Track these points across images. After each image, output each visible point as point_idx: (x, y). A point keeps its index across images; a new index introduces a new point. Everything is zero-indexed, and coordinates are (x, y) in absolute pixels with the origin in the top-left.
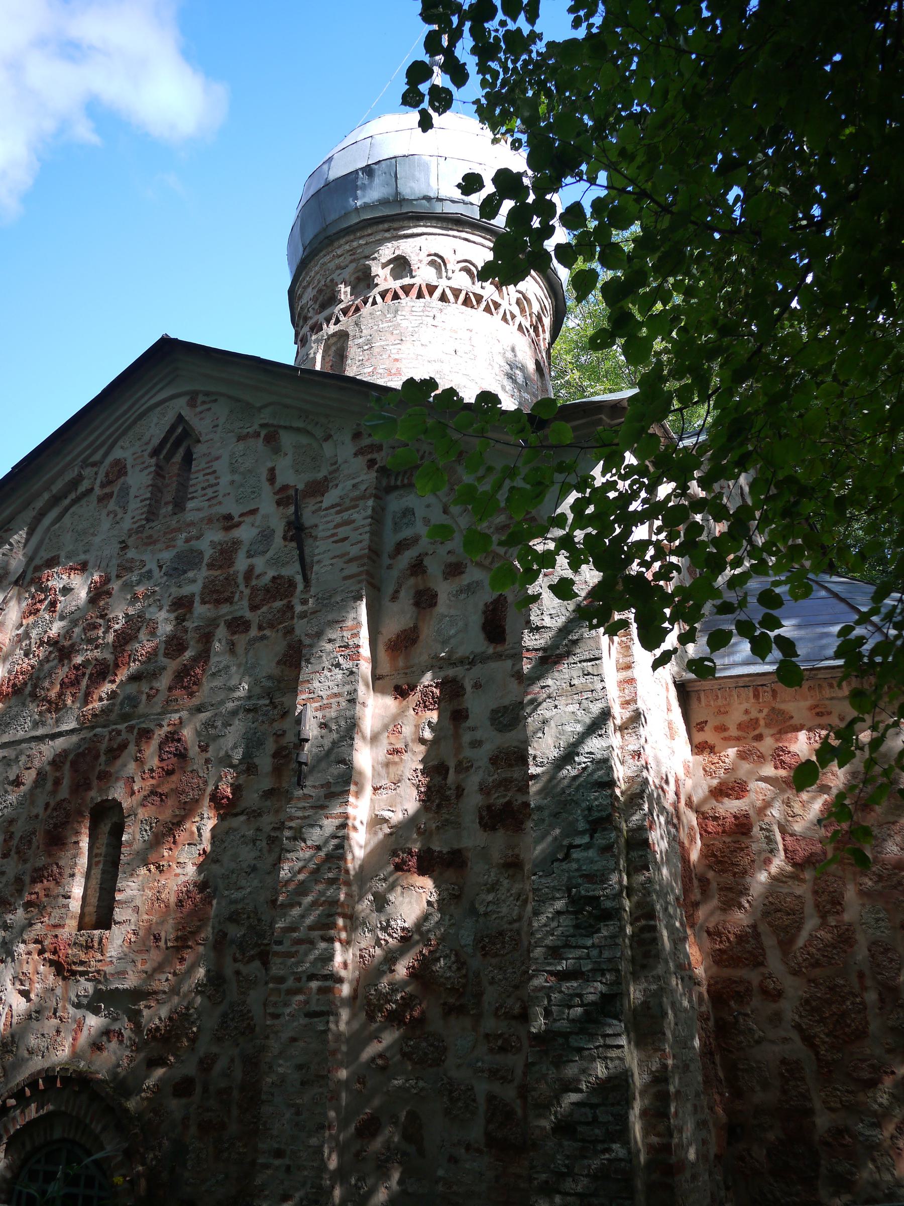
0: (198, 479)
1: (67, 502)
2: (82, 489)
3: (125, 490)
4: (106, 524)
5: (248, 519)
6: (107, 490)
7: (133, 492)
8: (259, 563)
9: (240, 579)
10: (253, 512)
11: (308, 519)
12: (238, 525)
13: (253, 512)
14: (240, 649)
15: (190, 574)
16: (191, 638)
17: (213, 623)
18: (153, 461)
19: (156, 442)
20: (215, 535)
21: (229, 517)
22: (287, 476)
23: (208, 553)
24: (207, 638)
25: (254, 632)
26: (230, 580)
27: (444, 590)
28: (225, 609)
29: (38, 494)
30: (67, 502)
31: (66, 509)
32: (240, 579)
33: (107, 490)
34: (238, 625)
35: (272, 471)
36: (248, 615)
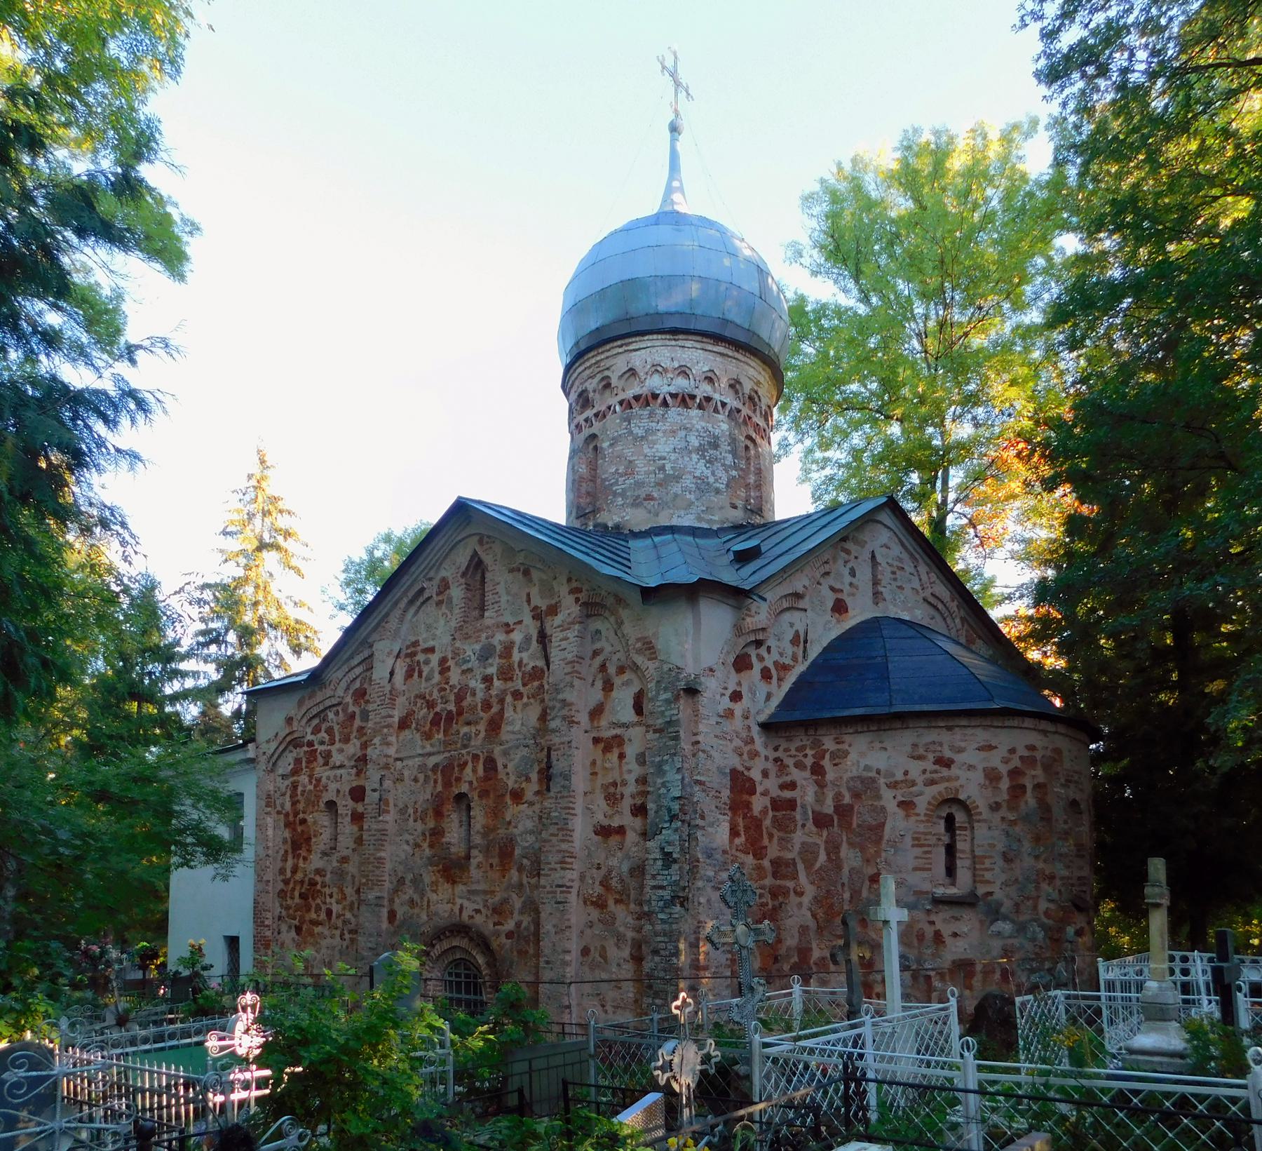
0: (489, 598)
1: (418, 603)
2: (426, 595)
3: (450, 599)
4: (442, 622)
5: (518, 627)
6: (440, 598)
7: (455, 601)
8: (525, 655)
9: (516, 666)
10: (520, 622)
11: (549, 631)
12: (512, 630)
13: (520, 622)
14: (519, 709)
15: (490, 661)
16: (494, 701)
17: (504, 692)
18: (463, 581)
19: (463, 568)
20: (500, 637)
21: (507, 625)
22: (537, 601)
23: (499, 648)
24: (502, 701)
25: (525, 700)
26: (511, 667)
27: (618, 681)
28: (510, 684)
29: (401, 599)
30: (418, 603)
31: (420, 607)
32: (516, 666)
33: (440, 598)
34: (517, 695)
35: (528, 595)
36: (521, 689)
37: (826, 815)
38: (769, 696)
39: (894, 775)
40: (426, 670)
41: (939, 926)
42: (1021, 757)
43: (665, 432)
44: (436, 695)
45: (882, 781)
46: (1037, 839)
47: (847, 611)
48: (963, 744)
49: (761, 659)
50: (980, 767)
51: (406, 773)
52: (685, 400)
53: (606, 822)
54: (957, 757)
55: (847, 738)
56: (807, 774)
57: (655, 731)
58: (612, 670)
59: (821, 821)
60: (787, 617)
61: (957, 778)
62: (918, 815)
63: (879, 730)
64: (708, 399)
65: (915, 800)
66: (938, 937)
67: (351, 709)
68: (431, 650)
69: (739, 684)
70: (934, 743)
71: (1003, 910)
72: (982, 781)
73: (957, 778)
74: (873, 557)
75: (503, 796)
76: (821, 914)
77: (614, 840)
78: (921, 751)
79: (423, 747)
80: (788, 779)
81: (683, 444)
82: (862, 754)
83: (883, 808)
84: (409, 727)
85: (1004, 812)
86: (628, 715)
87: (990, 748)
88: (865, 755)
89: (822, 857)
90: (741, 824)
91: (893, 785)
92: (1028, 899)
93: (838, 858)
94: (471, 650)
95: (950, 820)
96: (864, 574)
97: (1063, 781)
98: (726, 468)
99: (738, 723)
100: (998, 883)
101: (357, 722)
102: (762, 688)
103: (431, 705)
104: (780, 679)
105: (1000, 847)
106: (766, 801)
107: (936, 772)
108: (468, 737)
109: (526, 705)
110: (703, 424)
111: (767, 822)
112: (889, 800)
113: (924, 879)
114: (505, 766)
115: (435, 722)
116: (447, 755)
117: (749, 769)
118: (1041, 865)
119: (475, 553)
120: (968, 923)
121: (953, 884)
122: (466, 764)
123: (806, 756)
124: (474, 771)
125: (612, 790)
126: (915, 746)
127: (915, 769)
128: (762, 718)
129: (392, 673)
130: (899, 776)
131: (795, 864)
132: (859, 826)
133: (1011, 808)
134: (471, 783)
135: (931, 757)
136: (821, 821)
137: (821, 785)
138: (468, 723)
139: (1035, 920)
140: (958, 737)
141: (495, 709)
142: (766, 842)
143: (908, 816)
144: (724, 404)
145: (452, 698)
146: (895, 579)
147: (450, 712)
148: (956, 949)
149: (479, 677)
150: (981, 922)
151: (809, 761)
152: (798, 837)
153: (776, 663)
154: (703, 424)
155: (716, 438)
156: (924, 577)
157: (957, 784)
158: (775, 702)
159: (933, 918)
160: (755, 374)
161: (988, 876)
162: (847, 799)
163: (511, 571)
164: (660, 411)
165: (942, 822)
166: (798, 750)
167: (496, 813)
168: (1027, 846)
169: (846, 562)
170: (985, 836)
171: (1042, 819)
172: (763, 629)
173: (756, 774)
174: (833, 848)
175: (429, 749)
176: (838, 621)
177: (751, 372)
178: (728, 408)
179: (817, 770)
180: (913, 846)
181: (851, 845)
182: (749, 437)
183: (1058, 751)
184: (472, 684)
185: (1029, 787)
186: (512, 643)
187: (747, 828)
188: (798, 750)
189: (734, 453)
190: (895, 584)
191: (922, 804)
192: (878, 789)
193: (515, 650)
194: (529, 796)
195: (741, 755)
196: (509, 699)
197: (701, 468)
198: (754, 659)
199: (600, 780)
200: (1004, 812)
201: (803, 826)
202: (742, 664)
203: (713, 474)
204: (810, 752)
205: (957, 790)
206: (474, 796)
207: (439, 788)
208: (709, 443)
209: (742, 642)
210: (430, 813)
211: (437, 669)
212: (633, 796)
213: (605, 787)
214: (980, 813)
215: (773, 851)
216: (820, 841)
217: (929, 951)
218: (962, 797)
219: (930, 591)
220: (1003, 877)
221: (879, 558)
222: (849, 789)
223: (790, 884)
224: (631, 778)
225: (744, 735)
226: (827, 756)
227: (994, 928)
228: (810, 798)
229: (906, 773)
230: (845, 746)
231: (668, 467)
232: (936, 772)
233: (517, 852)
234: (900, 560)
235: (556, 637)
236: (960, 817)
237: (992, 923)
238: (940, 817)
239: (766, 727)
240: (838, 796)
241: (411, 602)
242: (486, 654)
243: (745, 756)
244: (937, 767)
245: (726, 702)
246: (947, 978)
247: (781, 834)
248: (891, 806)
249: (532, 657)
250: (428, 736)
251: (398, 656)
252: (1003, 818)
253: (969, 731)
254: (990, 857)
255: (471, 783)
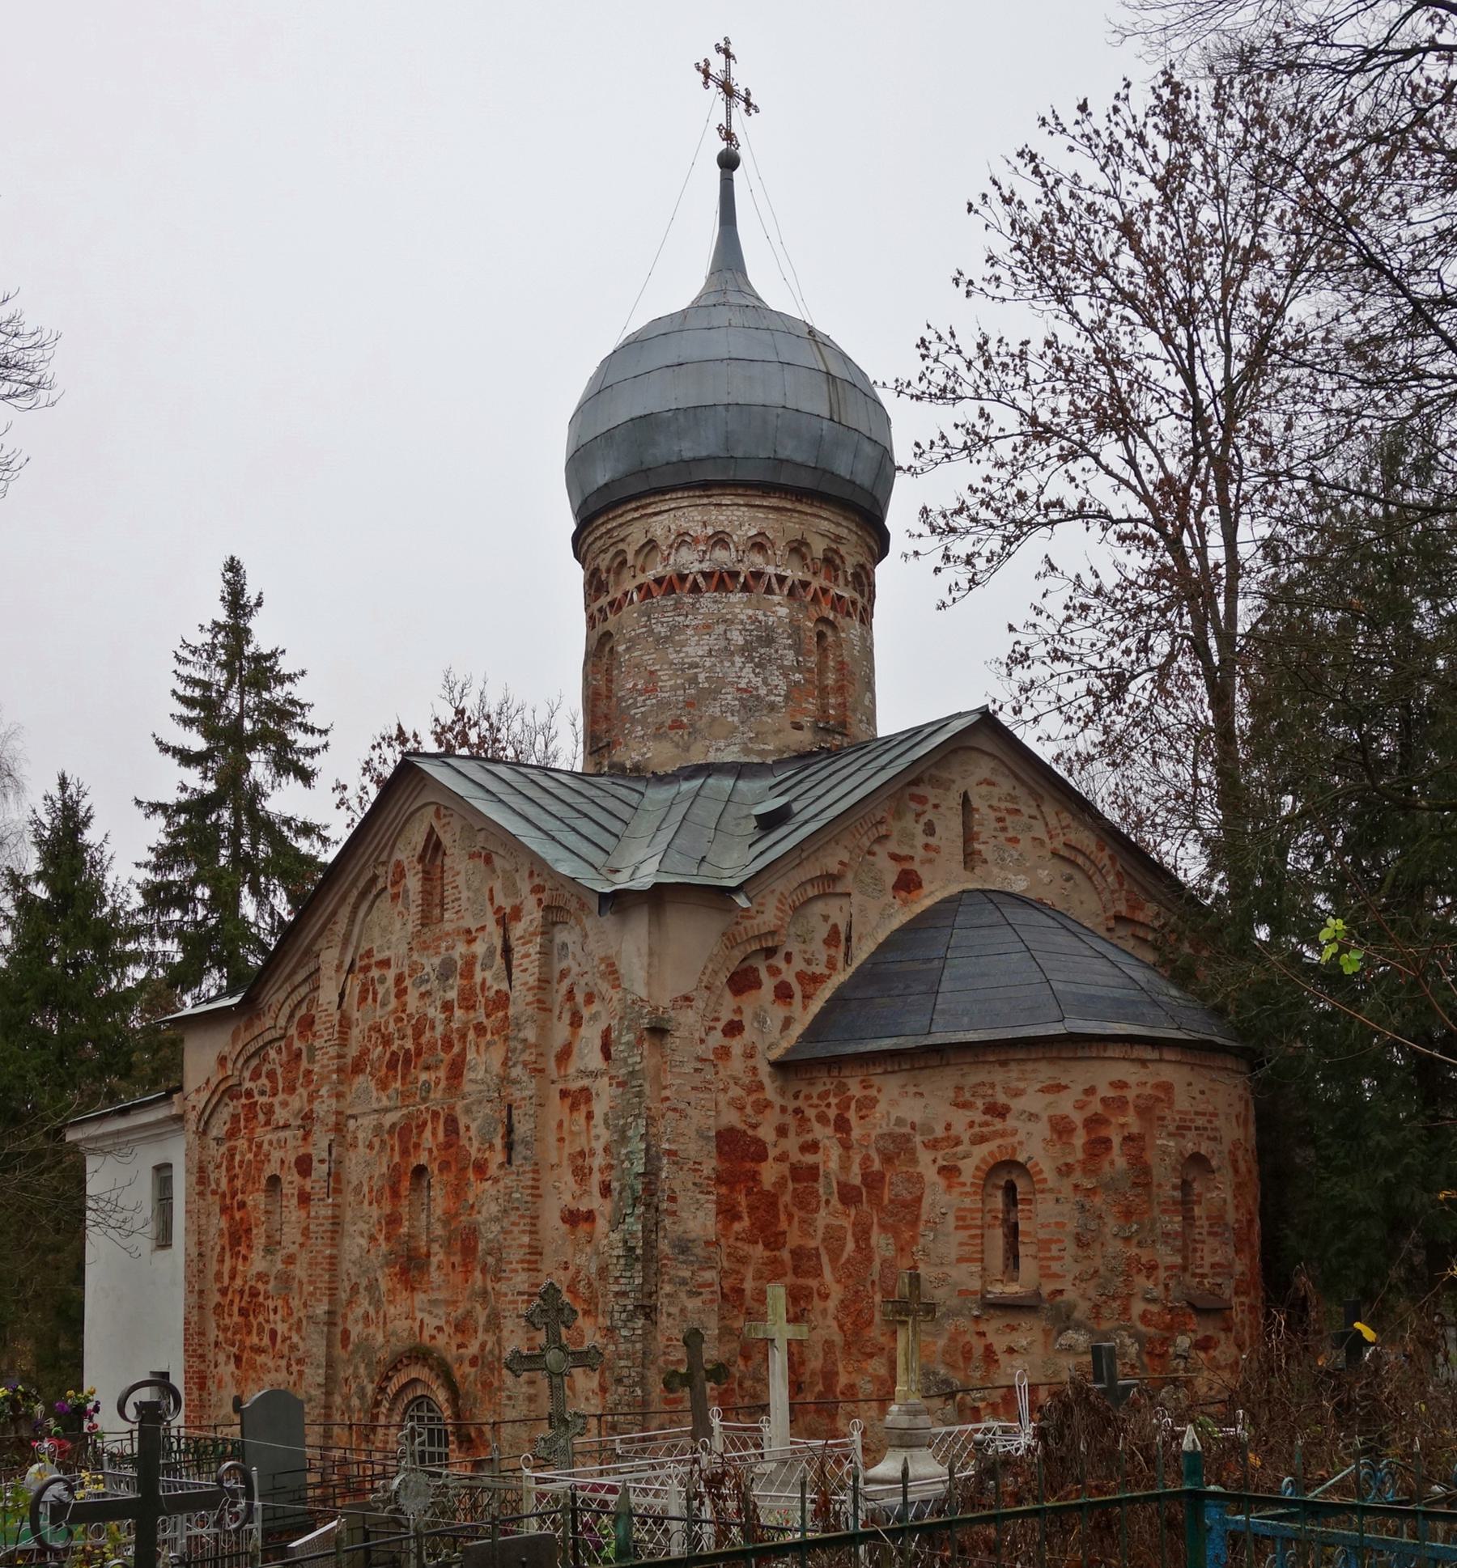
5: (480, 935)
8: (488, 974)
12: (474, 940)
19: (420, 848)
20: (461, 948)
21: (469, 931)
25: (489, 1037)
28: (472, 1014)
34: (480, 1029)
36: (485, 1021)
37: (855, 1187)
38: (787, 1023)
39: (932, 1130)
40: (381, 990)
42: (1103, 1100)
43: (696, 628)
44: (392, 1027)
46: (1127, 1214)
47: (919, 885)
49: (774, 971)
50: (1045, 1117)
51: (361, 1135)
52: (722, 580)
53: (573, 1206)
55: (876, 1081)
56: (829, 1131)
57: (619, 1085)
58: (580, 998)
59: (848, 1196)
60: (819, 907)
61: (1015, 1132)
64: (757, 575)
65: (961, 1164)
67: (297, 1044)
68: (385, 964)
70: (983, 1084)
71: (1077, 1315)
72: (1048, 1134)
73: (1015, 1132)
74: (966, 800)
75: (464, 1169)
76: (848, 1322)
77: (583, 1228)
78: (967, 1095)
79: (379, 1100)
80: (809, 1137)
81: (723, 643)
82: (893, 1103)
83: (920, 1176)
84: (362, 1071)
85: (1077, 1177)
86: (595, 1061)
87: (1059, 1088)
88: (899, 1104)
89: (850, 1245)
90: (744, 1203)
91: (933, 1145)
92: (1114, 1298)
93: (868, 1245)
94: (431, 963)
95: (1010, 1189)
96: (950, 828)
97: (1172, 1128)
98: (785, 672)
99: (737, 1065)
100: (1070, 1277)
101: (304, 1064)
102: (778, 1013)
103: (387, 1041)
104: (807, 997)
105: (1071, 1227)
106: (784, 1168)
107: (986, 1124)
108: (427, 1087)
109: (489, 1044)
110: (750, 612)
111: (787, 1198)
112: (927, 1165)
114: (468, 1128)
115: (392, 1065)
116: (405, 1111)
117: (755, 1127)
118: (1134, 1251)
119: (432, 831)
120: (1028, 1334)
121: (1015, 1280)
122: (425, 1123)
123: (828, 1105)
124: (434, 1134)
125: (580, 1162)
126: (959, 1089)
127: (960, 1120)
128: (775, 1054)
129: (342, 996)
130: (940, 1132)
131: (818, 1256)
133: (1087, 1172)
134: (430, 1151)
135: (980, 1103)
136: (848, 1196)
137: (846, 1146)
138: (427, 1068)
139: (1124, 1328)
140: (1014, 1075)
141: (456, 1049)
142: (783, 1225)
143: (950, 1187)
144: (781, 580)
145: (409, 1032)
146: (1004, 829)
147: (407, 1051)
149: (438, 1003)
150: (1046, 1333)
151: (832, 1113)
152: (822, 1218)
153: (800, 976)
154: (750, 612)
155: (770, 629)
156: (1053, 821)
158: (797, 1030)
159: (983, 1327)
160: (832, 528)
161: (1055, 1267)
162: (877, 1165)
163: (472, 856)
164: (688, 600)
165: (999, 1194)
166: (820, 1097)
167: (458, 1191)
168: (1112, 1225)
169: (918, 815)
170: (1048, 1214)
171: (1135, 1185)
172: (772, 933)
173: (767, 1133)
174: (863, 1234)
175: (385, 1102)
176: (905, 903)
177: (825, 525)
178: (789, 582)
179: (842, 1125)
181: (883, 1227)
182: (823, 620)
183: (1167, 1088)
184: (432, 1012)
185: (1116, 1141)
186: (474, 957)
187: (752, 1209)
188: (820, 1097)
189: (798, 648)
190: (1002, 836)
191: (968, 1169)
192: (913, 1151)
193: (478, 968)
194: (493, 1169)
195: (742, 1109)
196: (471, 1035)
197: (748, 676)
198: (763, 974)
199: (567, 1150)
200: (1077, 1177)
201: (827, 1202)
202: (742, 982)
203: (765, 682)
204: (833, 1101)
205: (1014, 1149)
206: (434, 1168)
207: (397, 1159)
208: (759, 638)
209: (738, 954)
210: (387, 1193)
211: (393, 991)
212: (601, 1171)
213: (573, 1158)
214: (1045, 1180)
215: (794, 1239)
216: (847, 1224)
218: (1021, 1158)
219: (1062, 839)
220: (1076, 1269)
221: (976, 802)
223: (813, 1283)
224: (599, 1146)
226: (853, 1105)
227: (1063, 1340)
228: (833, 1165)
229: (948, 1127)
230: (873, 1092)
231: (701, 677)
232: (986, 1124)
233: (481, 1246)
234: (1013, 799)
235: (518, 950)
236: (1021, 1186)
237: (1060, 1334)
238: (998, 1187)
239: (783, 1067)
240: (867, 1159)
241: (363, 895)
242: (446, 971)
244: (988, 1118)
245: (717, 1038)
246: (1001, 1410)
247: (802, 1214)
248: (930, 1174)
249: (496, 978)
250: (383, 1085)
251: (350, 970)
252: (1076, 1186)
253: (1030, 1066)
254: (1060, 1241)
255: (430, 1151)
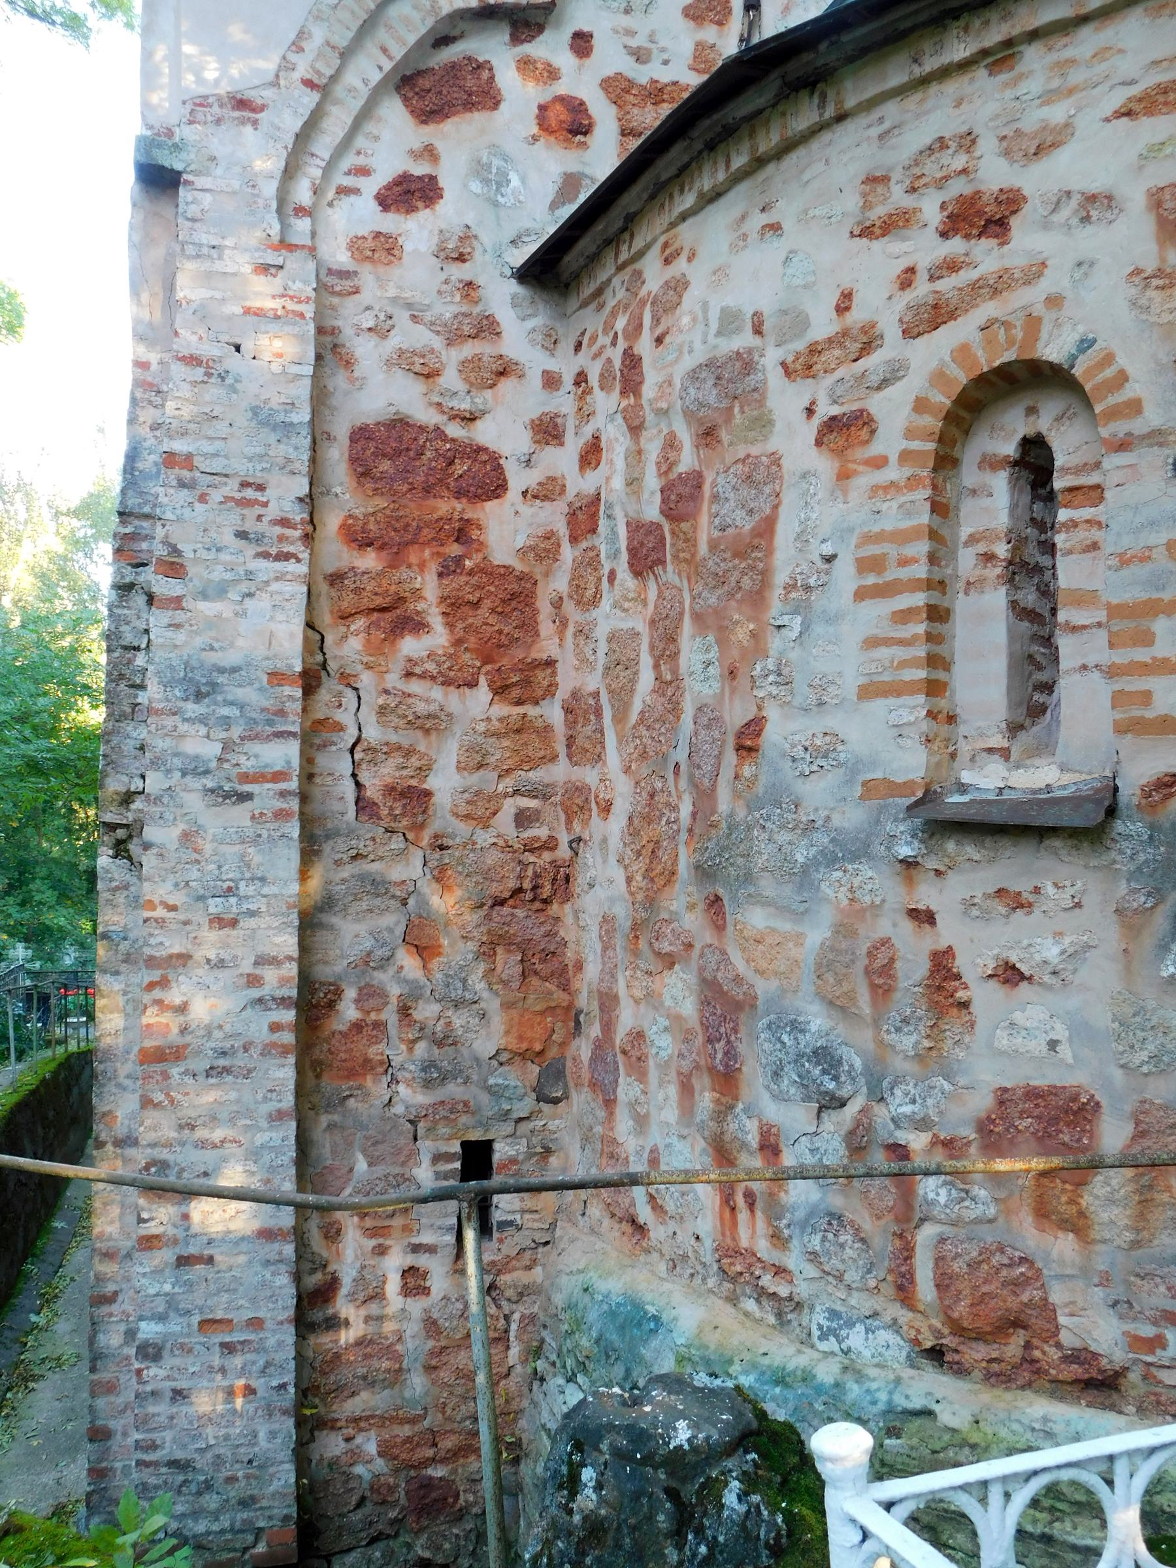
41: (948, 932)
45: (771, 358)
48: (1057, 113)
50: (1135, 197)
54: (1035, 180)
61: (1036, 271)
62: (880, 463)
63: (759, 163)
65: (876, 404)
66: (943, 968)
69: (429, 153)
73: (1036, 271)
78: (897, 197)
91: (802, 368)
107: (952, 266)
113: (900, 732)
127: (873, 270)
130: (823, 325)
132: (713, 546)
135: (931, 209)
140: (1033, 86)
143: (844, 476)
148: (1015, 1043)
157: (1031, 296)
159: (927, 895)
180: (861, 595)
192: (759, 393)
195: (430, 376)
205: (1033, 324)
214: (1134, 407)
217: (907, 1042)
218: (1053, 350)
222: (688, 414)
225: (448, 309)
232: (952, 266)
243: (451, 379)
244: (956, 245)
